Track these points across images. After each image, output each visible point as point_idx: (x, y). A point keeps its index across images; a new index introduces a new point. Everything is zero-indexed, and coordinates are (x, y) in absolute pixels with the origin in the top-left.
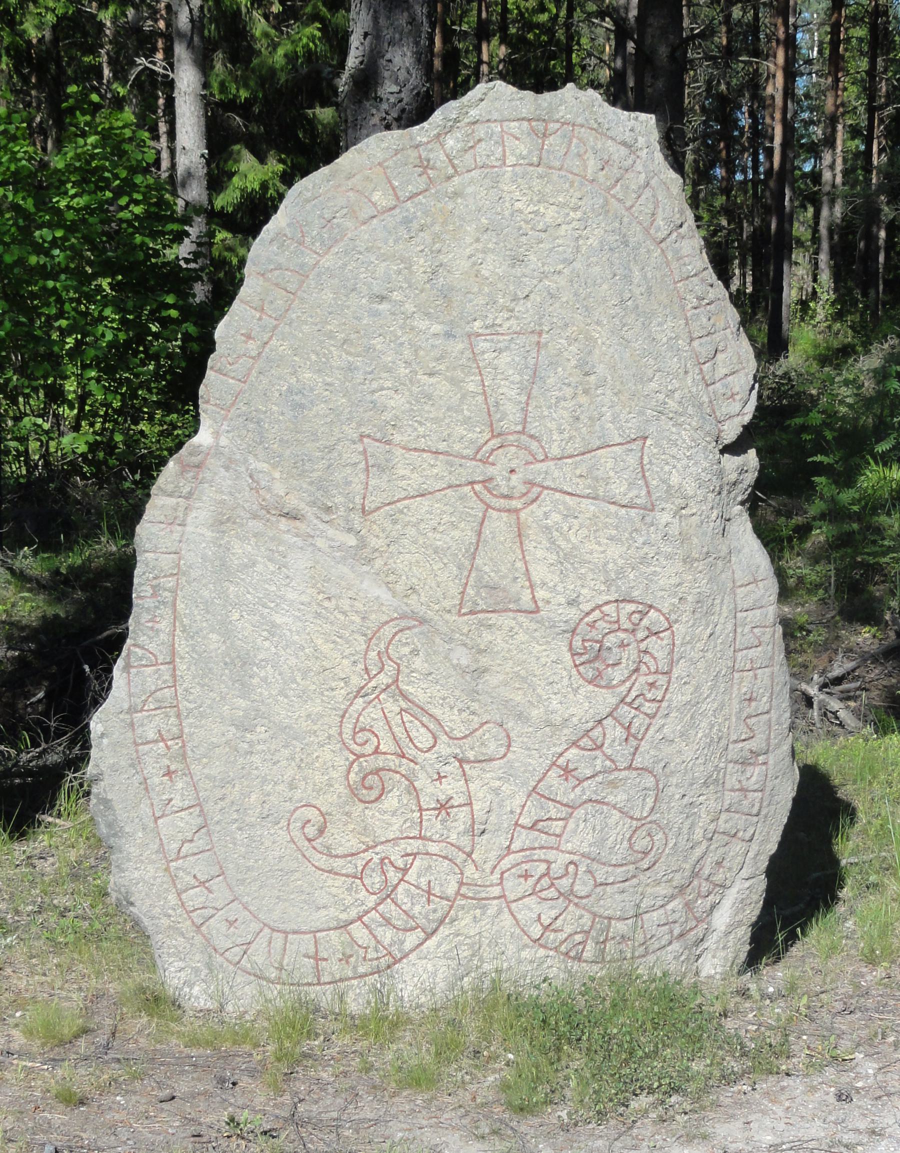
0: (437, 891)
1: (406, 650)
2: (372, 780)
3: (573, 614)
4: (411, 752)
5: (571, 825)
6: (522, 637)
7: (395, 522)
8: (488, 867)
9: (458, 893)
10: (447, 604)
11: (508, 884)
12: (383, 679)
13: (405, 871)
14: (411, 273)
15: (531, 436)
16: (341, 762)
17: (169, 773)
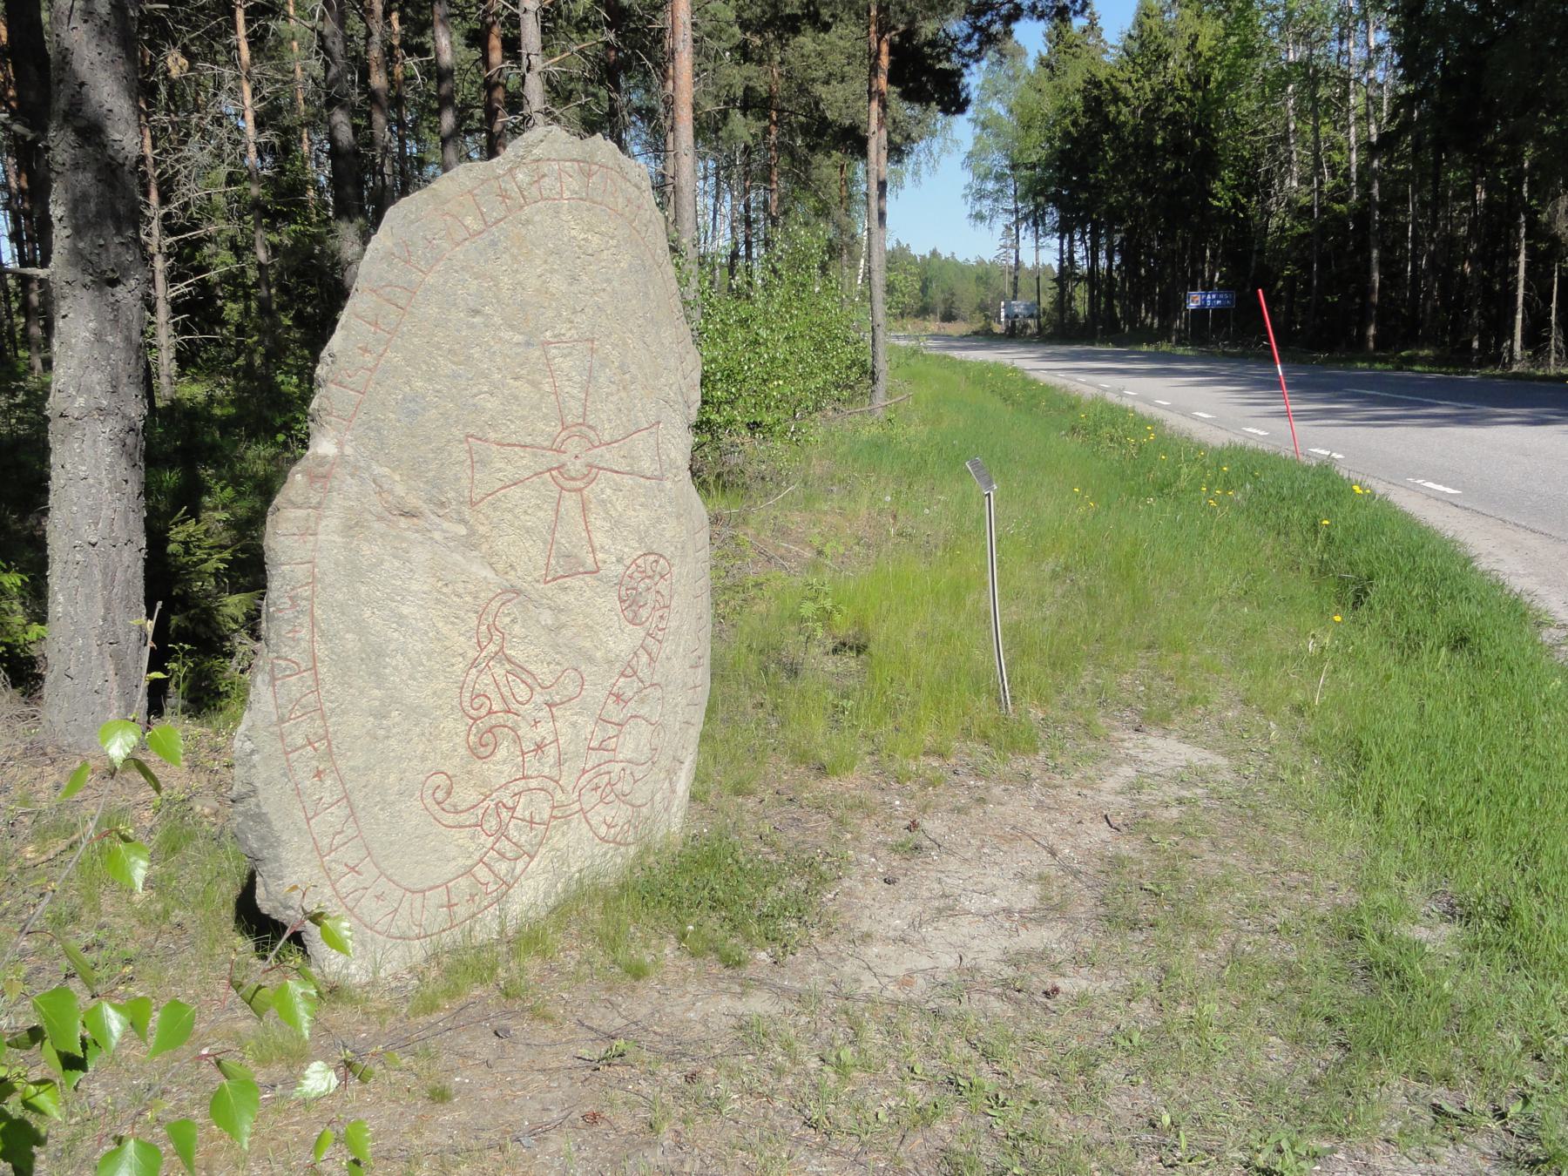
0: (537, 820)
1: (507, 620)
2: (488, 737)
3: (621, 569)
4: (514, 706)
5: (621, 739)
6: (588, 594)
7: (495, 509)
8: (570, 789)
9: (552, 817)
10: (536, 575)
11: (584, 799)
12: (492, 648)
13: (513, 809)
14: (500, 290)
15: (590, 427)
16: (462, 728)
17: (318, 774)
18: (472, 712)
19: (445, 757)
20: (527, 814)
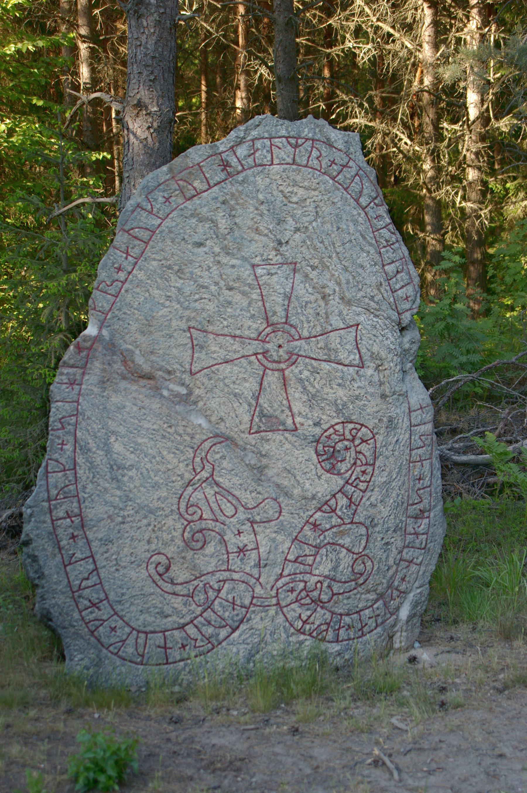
0: (238, 602)
1: (218, 456)
2: (198, 536)
3: (318, 431)
4: (222, 518)
5: (318, 559)
6: (287, 446)
7: (210, 379)
8: (269, 587)
9: (251, 603)
10: (242, 427)
11: (281, 596)
12: (205, 474)
13: (219, 591)
14: (218, 228)
15: (291, 326)
16: (179, 526)
17: (73, 537)
18: (187, 516)
19: (165, 544)
20: (230, 597)
